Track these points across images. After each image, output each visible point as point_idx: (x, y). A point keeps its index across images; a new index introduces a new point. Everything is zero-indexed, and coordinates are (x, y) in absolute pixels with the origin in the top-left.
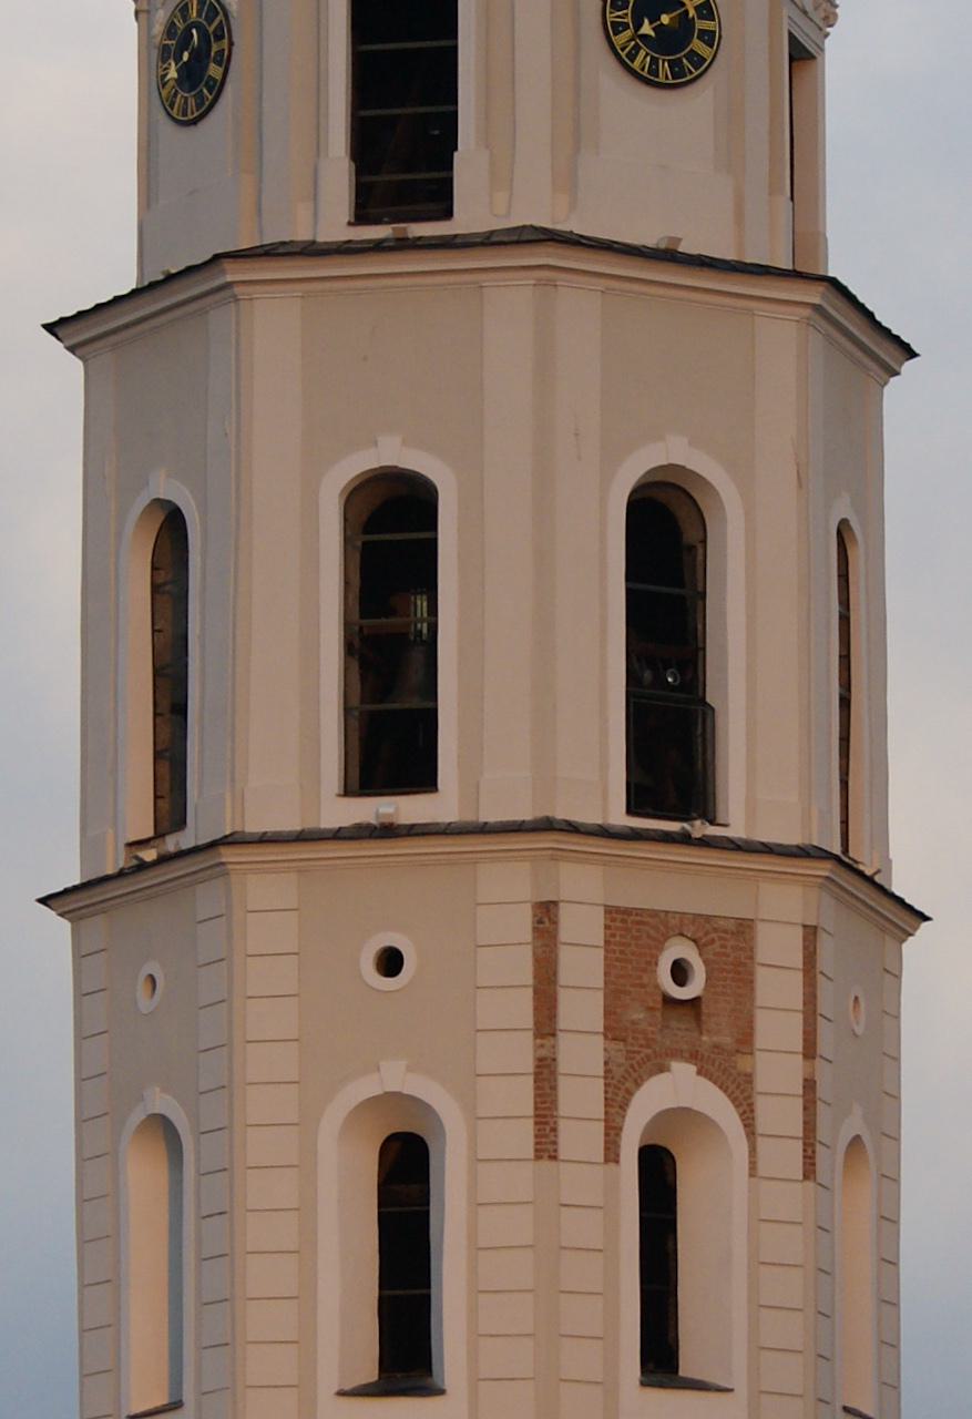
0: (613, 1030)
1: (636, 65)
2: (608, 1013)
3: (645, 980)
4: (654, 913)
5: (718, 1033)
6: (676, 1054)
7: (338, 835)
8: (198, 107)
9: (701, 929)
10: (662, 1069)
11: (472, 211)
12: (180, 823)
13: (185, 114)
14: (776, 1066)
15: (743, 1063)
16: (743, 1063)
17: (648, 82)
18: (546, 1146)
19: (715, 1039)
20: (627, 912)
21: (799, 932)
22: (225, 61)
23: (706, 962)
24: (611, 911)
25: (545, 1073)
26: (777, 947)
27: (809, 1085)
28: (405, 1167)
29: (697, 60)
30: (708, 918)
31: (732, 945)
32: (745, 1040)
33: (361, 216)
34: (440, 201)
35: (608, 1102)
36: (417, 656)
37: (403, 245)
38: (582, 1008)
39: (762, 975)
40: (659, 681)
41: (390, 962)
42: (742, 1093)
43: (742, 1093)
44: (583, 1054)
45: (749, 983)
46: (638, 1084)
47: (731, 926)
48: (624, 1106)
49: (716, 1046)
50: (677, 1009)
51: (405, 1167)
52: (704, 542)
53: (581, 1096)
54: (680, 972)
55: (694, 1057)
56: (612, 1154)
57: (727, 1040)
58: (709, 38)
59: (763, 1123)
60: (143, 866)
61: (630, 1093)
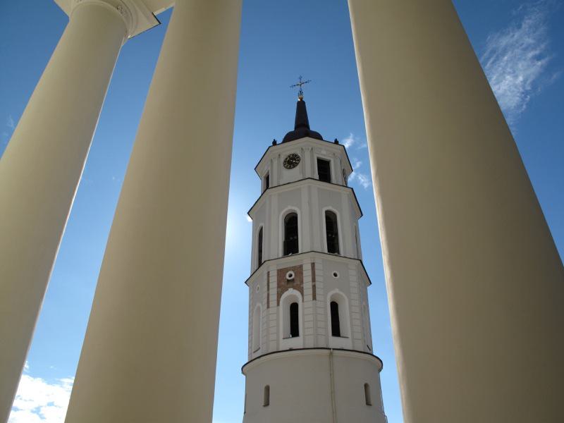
0: (279, 286)
2: (278, 284)
5: (298, 282)
6: (290, 287)
9: (293, 269)
14: (307, 285)
18: (268, 307)
27: (314, 287)
31: (299, 270)
32: (302, 282)
38: (274, 285)
39: (304, 273)
42: (302, 291)
43: (302, 291)
44: (274, 291)
45: (302, 273)
50: (289, 280)
53: (273, 297)
54: (291, 276)
56: (278, 304)
57: (299, 283)
59: (305, 294)
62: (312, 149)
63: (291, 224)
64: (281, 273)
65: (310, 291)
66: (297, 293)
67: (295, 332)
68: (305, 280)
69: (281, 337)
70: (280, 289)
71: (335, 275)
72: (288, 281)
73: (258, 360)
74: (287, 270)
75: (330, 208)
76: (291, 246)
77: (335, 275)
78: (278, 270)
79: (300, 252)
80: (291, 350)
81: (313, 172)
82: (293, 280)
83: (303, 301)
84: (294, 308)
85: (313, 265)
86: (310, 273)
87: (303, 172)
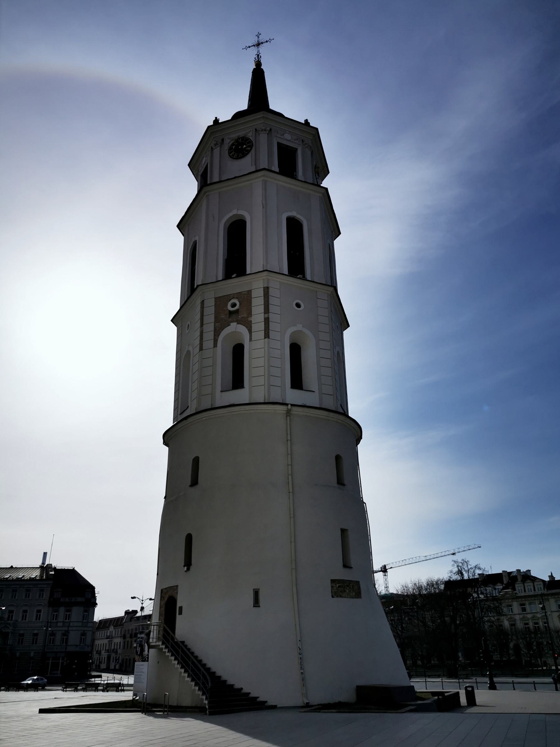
2: (215, 318)
9: (238, 296)
10: (229, 325)
15: (249, 319)
16: (249, 319)
23: (239, 302)
27: (267, 321)
32: (250, 314)
35: (215, 335)
38: (210, 319)
44: (210, 328)
47: (246, 293)
53: (209, 335)
54: (234, 305)
56: (215, 345)
57: (245, 315)
62: (271, 130)
63: (236, 232)
64: (220, 302)
65: (262, 326)
66: (242, 329)
67: (237, 381)
68: (254, 310)
69: (219, 388)
71: (298, 305)
72: (231, 313)
73: (185, 421)
74: (228, 297)
75: (294, 214)
76: (235, 264)
77: (298, 305)
78: (216, 298)
79: (247, 273)
81: (270, 161)
82: (237, 311)
83: (251, 340)
84: (238, 351)
85: (266, 290)
86: (261, 301)
87: (256, 161)
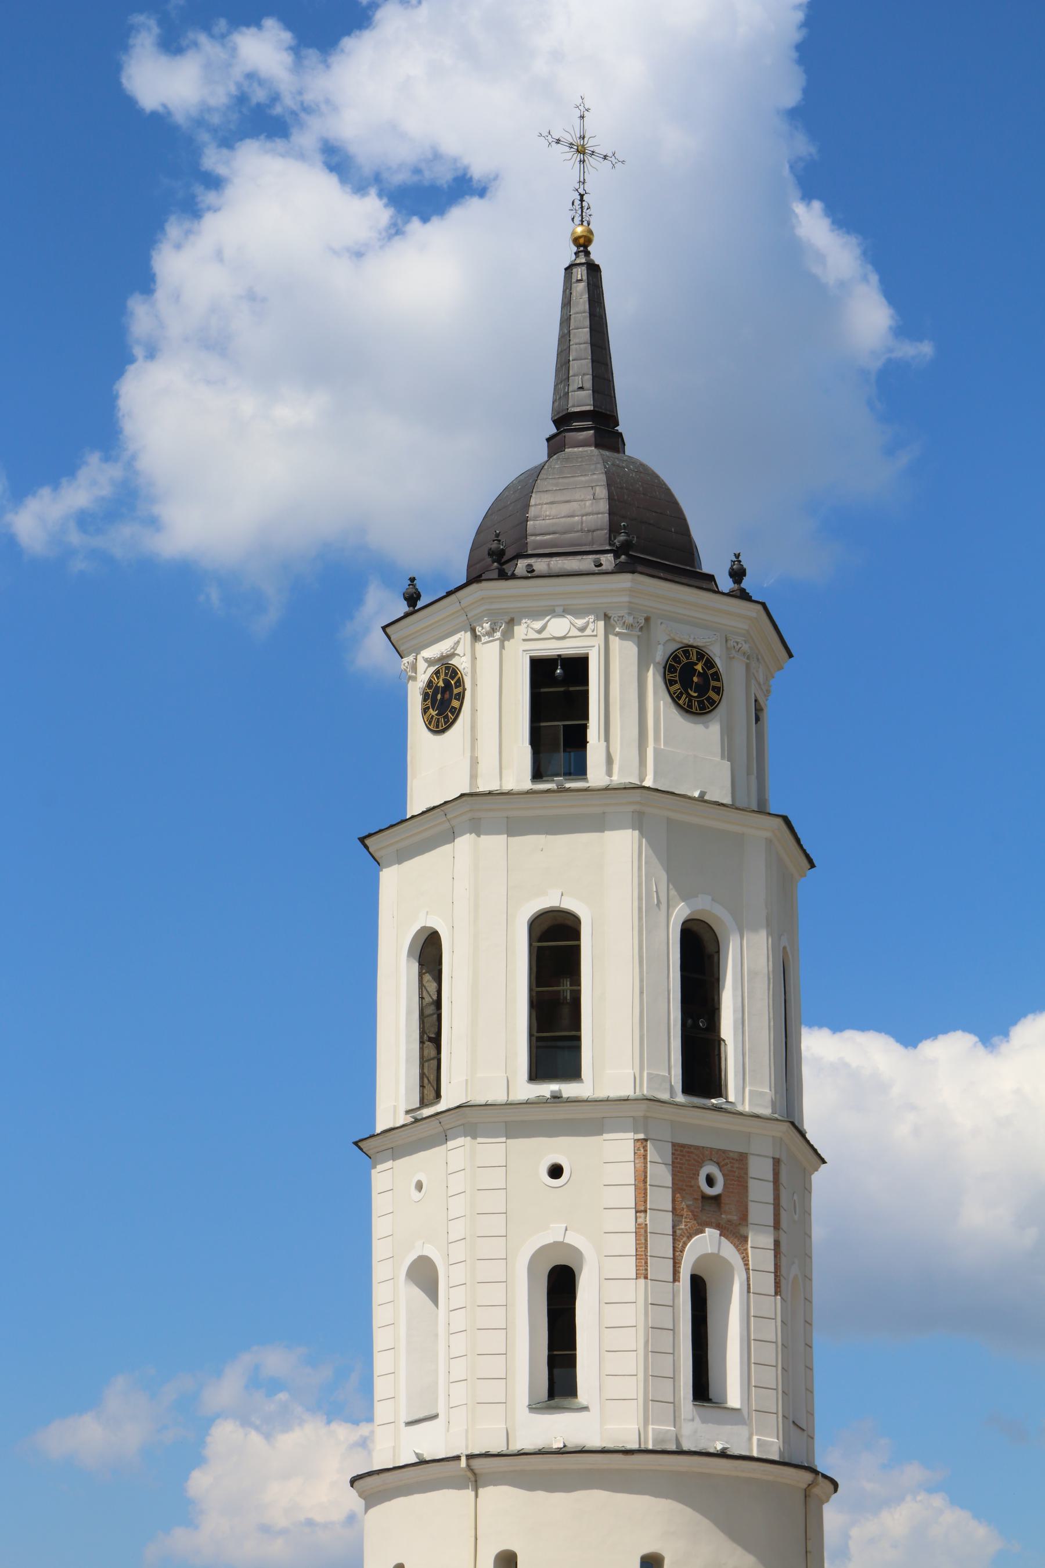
1: (681, 702)
3: (693, 1183)
4: (697, 1148)
5: (730, 1215)
6: (709, 1225)
7: (527, 1103)
8: (446, 723)
9: (721, 1158)
11: (596, 775)
12: (438, 1096)
13: (437, 727)
16: (743, 1231)
17: (687, 711)
18: (642, 1273)
19: (729, 1217)
20: (683, 1146)
21: (771, 1161)
22: (461, 697)
24: (674, 1145)
25: (642, 1233)
26: (759, 1169)
28: (561, 1285)
29: (712, 702)
30: (724, 1151)
32: (744, 1218)
33: (537, 775)
34: (580, 771)
36: (566, 1011)
37: (562, 790)
38: (662, 1198)
39: (752, 1184)
40: (696, 1025)
41: (556, 1172)
45: (746, 1188)
46: (690, 1238)
48: (682, 1251)
49: (729, 1221)
51: (561, 1285)
52: (718, 952)
53: (662, 1246)
54: (710, 1181)
55: (718, 1226)
56: (676, 1278)
57: (735, 1218)
58: (718, 690)
60: (416, 1121)
61: (685, 1244)
64: (685, 1160)
66: (729, 1251)
70: (676, 1218)
72: (705, 1198)
73: (620, 1456)
80: (723, 1454)
82: (716, 1198)
